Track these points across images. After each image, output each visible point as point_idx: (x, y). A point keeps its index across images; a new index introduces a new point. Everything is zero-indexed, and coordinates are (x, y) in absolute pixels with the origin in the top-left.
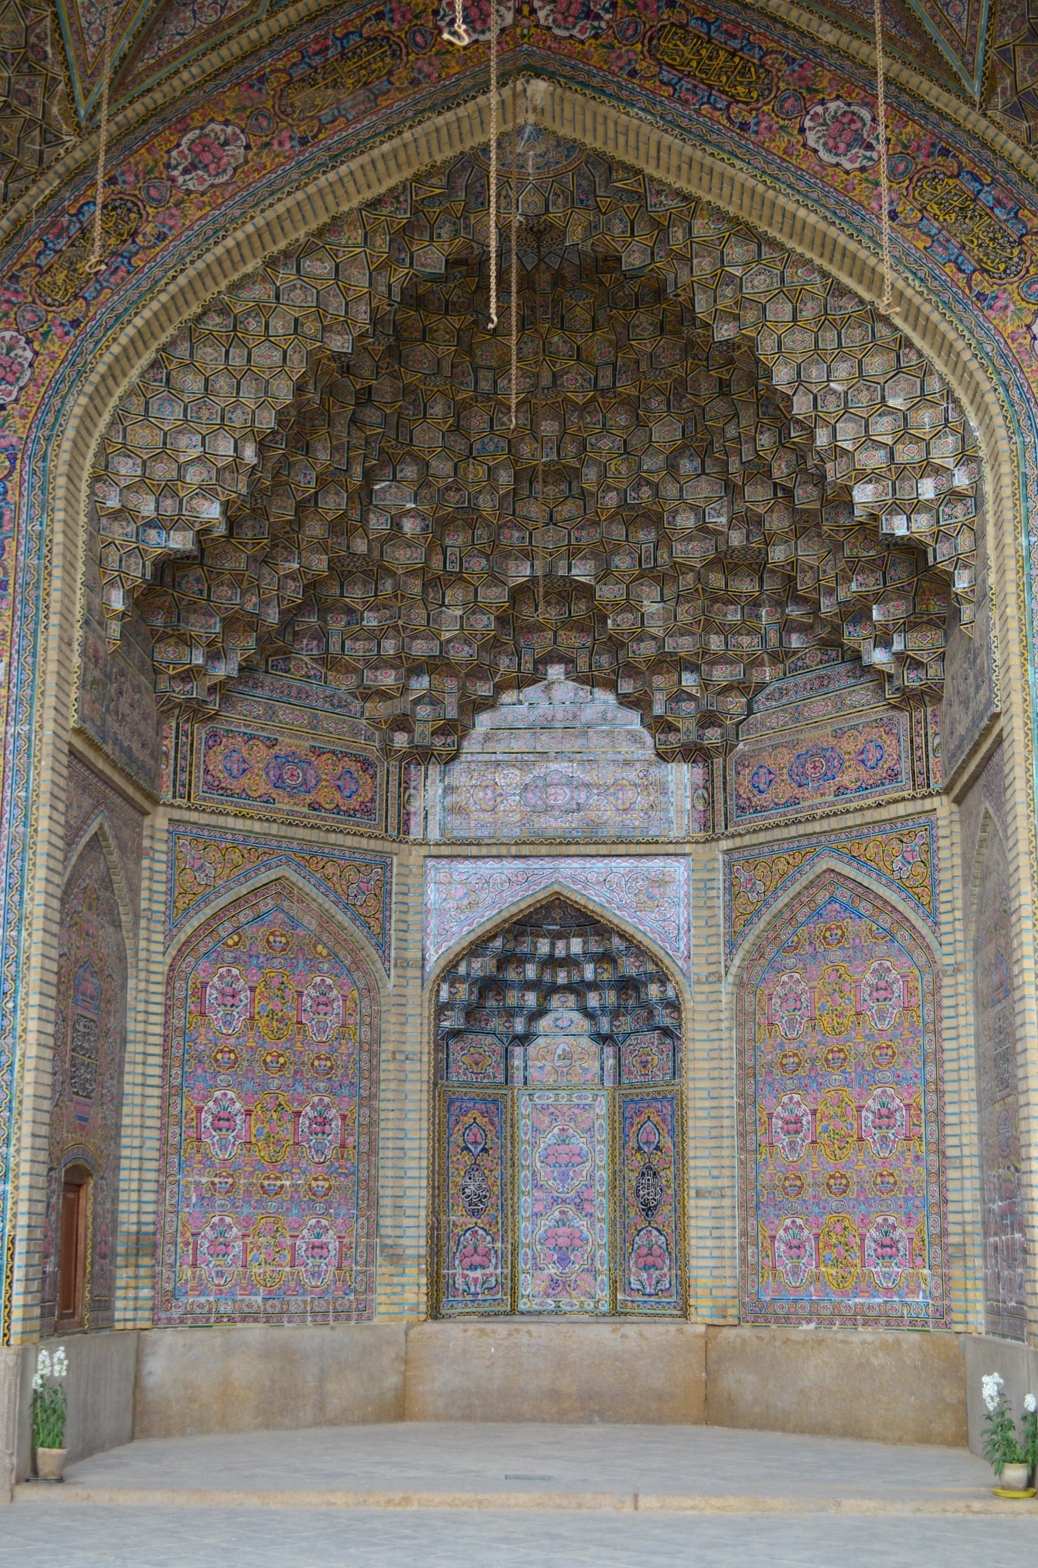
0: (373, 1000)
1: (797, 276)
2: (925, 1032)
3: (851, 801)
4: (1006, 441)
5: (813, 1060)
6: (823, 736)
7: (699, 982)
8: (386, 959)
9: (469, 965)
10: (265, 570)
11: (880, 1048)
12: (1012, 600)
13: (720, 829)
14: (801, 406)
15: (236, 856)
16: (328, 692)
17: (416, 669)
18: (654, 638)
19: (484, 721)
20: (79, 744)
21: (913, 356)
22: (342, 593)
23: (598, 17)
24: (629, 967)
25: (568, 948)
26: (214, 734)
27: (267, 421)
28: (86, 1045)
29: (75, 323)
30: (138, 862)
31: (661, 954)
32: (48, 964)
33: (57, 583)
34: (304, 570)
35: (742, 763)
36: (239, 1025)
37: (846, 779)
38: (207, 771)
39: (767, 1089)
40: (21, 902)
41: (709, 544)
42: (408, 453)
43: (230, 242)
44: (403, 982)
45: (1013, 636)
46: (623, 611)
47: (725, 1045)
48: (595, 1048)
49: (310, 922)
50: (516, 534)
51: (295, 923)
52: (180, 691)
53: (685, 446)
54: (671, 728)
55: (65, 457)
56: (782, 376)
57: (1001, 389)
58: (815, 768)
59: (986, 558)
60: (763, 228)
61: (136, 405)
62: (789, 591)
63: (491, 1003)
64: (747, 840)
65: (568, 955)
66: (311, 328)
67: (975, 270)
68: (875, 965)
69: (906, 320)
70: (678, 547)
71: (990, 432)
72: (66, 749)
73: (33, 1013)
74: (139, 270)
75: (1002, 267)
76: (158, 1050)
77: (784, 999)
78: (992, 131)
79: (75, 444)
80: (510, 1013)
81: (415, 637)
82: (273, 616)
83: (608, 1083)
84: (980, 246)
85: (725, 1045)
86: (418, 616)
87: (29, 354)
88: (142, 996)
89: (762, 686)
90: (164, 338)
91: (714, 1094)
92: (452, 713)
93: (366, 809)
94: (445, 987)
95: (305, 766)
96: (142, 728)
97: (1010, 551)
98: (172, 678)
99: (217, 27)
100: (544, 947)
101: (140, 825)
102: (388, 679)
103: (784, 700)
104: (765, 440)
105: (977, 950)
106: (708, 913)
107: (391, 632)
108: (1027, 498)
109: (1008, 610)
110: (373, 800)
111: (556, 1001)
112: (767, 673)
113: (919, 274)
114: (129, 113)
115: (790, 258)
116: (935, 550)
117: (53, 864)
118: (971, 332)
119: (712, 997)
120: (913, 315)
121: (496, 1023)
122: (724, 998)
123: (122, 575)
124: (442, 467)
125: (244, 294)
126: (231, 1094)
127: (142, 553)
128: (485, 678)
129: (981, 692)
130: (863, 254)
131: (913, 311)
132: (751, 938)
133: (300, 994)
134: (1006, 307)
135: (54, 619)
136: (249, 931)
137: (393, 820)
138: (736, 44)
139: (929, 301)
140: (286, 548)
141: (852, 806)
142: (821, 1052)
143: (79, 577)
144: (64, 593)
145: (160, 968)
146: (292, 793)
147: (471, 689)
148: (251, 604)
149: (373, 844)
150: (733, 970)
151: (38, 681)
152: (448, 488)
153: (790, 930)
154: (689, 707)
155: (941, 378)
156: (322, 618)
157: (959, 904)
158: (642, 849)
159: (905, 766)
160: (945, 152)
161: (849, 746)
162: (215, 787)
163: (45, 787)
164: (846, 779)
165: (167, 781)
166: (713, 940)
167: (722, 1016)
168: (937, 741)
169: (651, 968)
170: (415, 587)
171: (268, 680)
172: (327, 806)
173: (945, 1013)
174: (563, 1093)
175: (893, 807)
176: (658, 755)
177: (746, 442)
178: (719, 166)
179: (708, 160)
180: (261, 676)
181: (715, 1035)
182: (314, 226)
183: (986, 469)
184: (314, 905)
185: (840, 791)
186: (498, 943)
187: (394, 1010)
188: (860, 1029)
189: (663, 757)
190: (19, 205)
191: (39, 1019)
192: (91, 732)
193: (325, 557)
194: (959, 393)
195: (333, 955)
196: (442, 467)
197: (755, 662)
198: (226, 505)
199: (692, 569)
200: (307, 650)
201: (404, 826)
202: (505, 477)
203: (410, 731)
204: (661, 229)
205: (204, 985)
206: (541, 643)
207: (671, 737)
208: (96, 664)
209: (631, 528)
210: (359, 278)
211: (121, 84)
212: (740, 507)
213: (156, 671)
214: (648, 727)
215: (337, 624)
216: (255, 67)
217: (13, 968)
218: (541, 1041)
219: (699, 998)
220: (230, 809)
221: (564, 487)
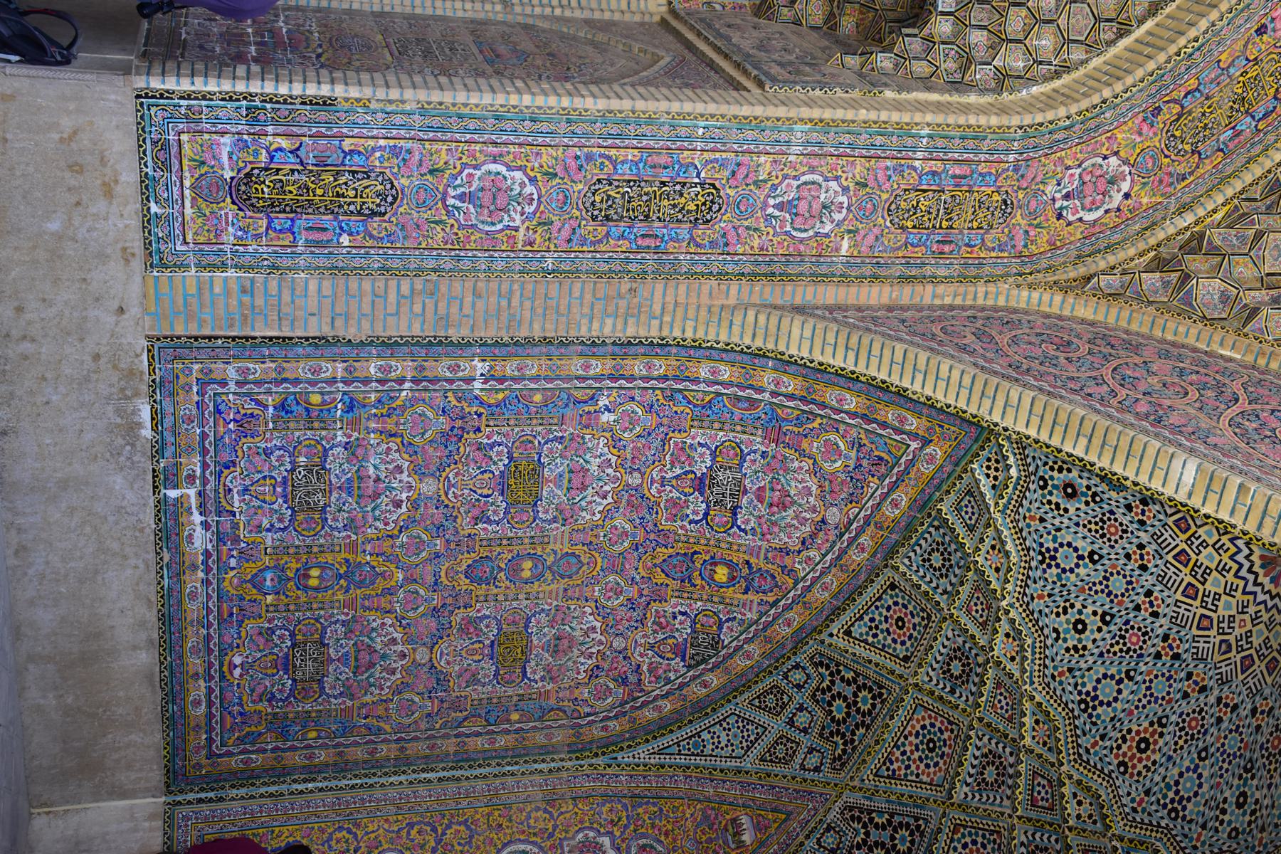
4: (1018, 123)
12: (873, 115)
21: (1109, 35)
45: (839, 114)
57: (1068, 123)
67: (1182, 107)
69: (1149, 33)
71: (1028, 107)
75: (1178, 134)
84: (1203, 114)
97: (918, 118)
105: (526, 27)
108: (962, 138)
109: (864, 111)
113: (1197, 53)
116: (915, 36)
118: (1127, 99)
120: (1152, 44)
129: (778, 69)
131: (1159, 43)
134: (1140, 134)
139: (1168, 61)
157: (568, 13)
183: (989, 98)
194: (1066, 79)
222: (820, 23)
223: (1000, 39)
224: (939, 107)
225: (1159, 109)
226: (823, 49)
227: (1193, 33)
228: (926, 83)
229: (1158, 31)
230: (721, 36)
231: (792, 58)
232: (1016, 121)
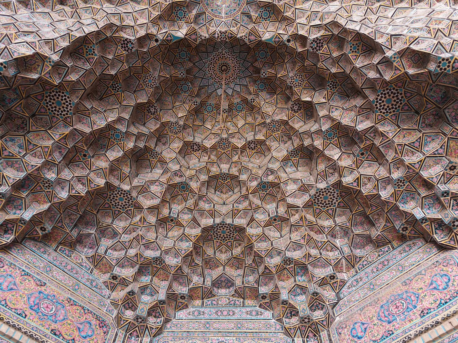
3: (436, 315)
16: (91, 277)
19: (181, 314)
22: (112, 223)
27: (78, 35)
46: (261, 240)
50: (207, 205)
56: (351, 26)
58: (397, 307)
81: (147, 246)
89: (343, 283)
95: (59, 306)
102: (127, 272)
103: (361, 283)
140: (83, 168)
141: (439, 318)
146: (43, 317)
170: (152, 219)
171: (54, 254)
172: (66, 337)
177: (324, 124)
180: (51, 251)
206: (216, 273)
209: (263, 203)
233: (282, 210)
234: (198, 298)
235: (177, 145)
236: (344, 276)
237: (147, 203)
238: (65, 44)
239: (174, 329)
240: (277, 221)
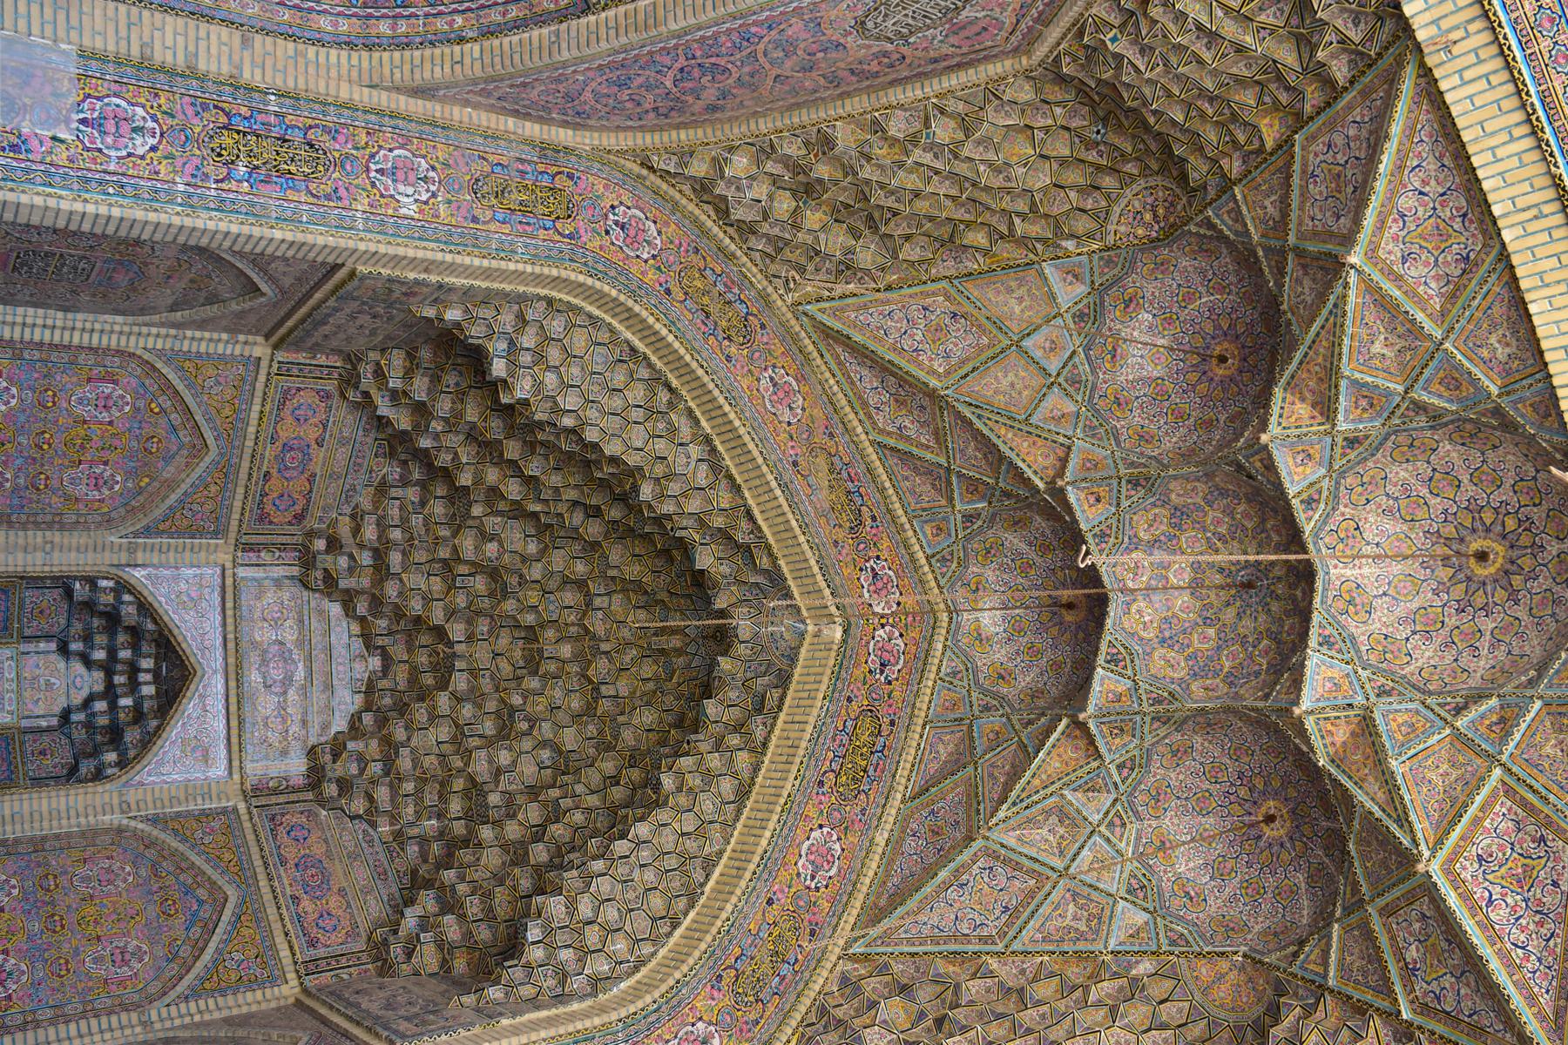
0: (100, 524)
1: (715, 832)
2: (84, 1003)
5: (53, 903)
6: (339, 880)
7: (121, 795)
8: (136, 535)
9: (130, 603)
10: (462, 437)
11: (67, 962)
13: (254, 802)
14: (621, 847)
15: (227, 412)
17: (379, 555)
18: (409, 739)
19: (335, 609)
20: (341, 274)
21: (666, 929)
23: (882, 672)
24: (131, 736)
25: (146, 683)
26: (328, 396)
27: (591, 435)
28: (65, 270)
29: (668, 292)
30: (226, 330)
31: (145, 762)
32: (149, 229)
33: (477, 262)
34: (459, 467)
35: (310, 814)
36: (79, 410)
37: (306, 904)
38: (299, 389)
39: (23, 864)
40: (209, 209)
41: (486, 777)
42: (547, 546)
43: (727, 408)
44: (116, 549)
47: (64, 822)
48: (57, 709)
49: (168, 472)
51: (168, 459)
52: (366, 371)
53: (560, 752)
54: (336, 756)
55: (573, 276)
56: (642, 830)
59: (522, 1013)
60: (749, 804)
61: (604, 336)
62: (454, 845)
63: (96, 622)
64: (247, 825)
65: (140, 684)
66: (659, 470)
68: (145, 948)
69: (694, 921)
70: (483, 753)
71: (622, 1001)
72: (339, 261)
73: (103, 210)
74: (706, 341)
76: (57, 339)
77: (109, 870)
78: (829, 966)
79: (581, 285)
80: (87, 638)
81: (404, 553)
82: (425, 443)
83: (25, 723)
85: (64, 822)
86: (421, 556)
87: (645, 256)
88: (107, 327)
89: (374, 825)
90: (653, 358)
91: (17, 818)
92: (343, 584)
93: (263, 518)
94: (111, 584)
96: (342, 336)
98: (378, 364)
99: (865, 404)
100: (147, 663)
101: (256, 334)
102: (370, 533)
104: (578, 817)
106: (182, 798)
107: (407, 536)
110: (271, 523)
111: (99, 675)
112: (385, 828)
114: (807, 341)
115: (728, 826)
117: (242, 240)
119: (108, 808)
121: (78, 627)
122: (107, 818)
123: (473, 320)
124: (536, 572)
125: (683, 420)
126: (14, 402)
127: (489, 337)
128: (370, 609)
129: (406, 1024)
130: (743, 884)
131: (704, 927)
132: (163, 836)
133: (106, 463)
135: (449, 258)
136: (163, 421)
137: (254, 539)
138: (871, 772)
141: (284, 911)
142: (61, 909)
143: (477, 283)
144: (466, 266)
145: (133, 345)
146: (280, 459)
147: (362, 598)
148: (437, 426)
149: (234, 523)
150: (133, 823)
151: (400, 240)
152: (521, 576)
153: (172, 869)
154: (354, 769)
155: (654, 954)
156: (418, 483)
157: (207, 1017)
158: (234, 740)
159: (321, 952)
160: (813, 933)
161: (334, 902)
162: (286, 396)
163: (310, 239)
164: (306, 904)
165: (292, 357)
166: (159, 804)
167: (91, 818)
168: (345, 977)
169: (132, 753)
170: (444, 553)
171: (369, 440)
173: (104, 1019)
174: (14, 685)
175: (286, 946)
176: (313, 747)
178: (794, 768)
179: (798, 760)
180: (373, 435)
181: (72, 813)
182: (734, 471)
183: (589, 1002)
184: (183, 476)
185: (296, 899)
186: (150, 626)
187: (91, 542)
188: (84, 941)
189: (312, 752)
190: (745, 259)
191: (97, 215)
192: (349, 287)
193: (469, 483)
194: (644, 971)
195: (141, 491)
196: (536, 572)
197: (394, 818)
198: (525, 403)
199: (467, 764)
200: (393, 471)
201: (249, 548)
202: (530, 619)
203: (327, 551)
204: (738, 727)
205: (115, 382)
206: (399, 651)
207: (328, 757)
208: (405, 294)
210: (694, 505)
211: (828, 336)
212: (520, 799)
213: (383, 350)
214: (335, 738)
215: (412, 494)
216: (839, 430)
217: (146, 196)
218: (62, 665)
219: (107, 796)
220: (268, 408)
221: (521, 664)
222: (436, 970)
223: (584, 953)
224: (550, 1022)
225: (720, 976)
226: (442, 994)
227: (724, 915)
228: (535, 1003)
229: (700, 918)
230: (350, 1004)
231: (416, 1009)
232: (614, 1016)
233: (475, 742)
234: (363, 628)
235: (580, 568)
236: (385, 828)
237: (467, 544)
238: (568, 421)
239: (313, 604)
240: (460, 733)
